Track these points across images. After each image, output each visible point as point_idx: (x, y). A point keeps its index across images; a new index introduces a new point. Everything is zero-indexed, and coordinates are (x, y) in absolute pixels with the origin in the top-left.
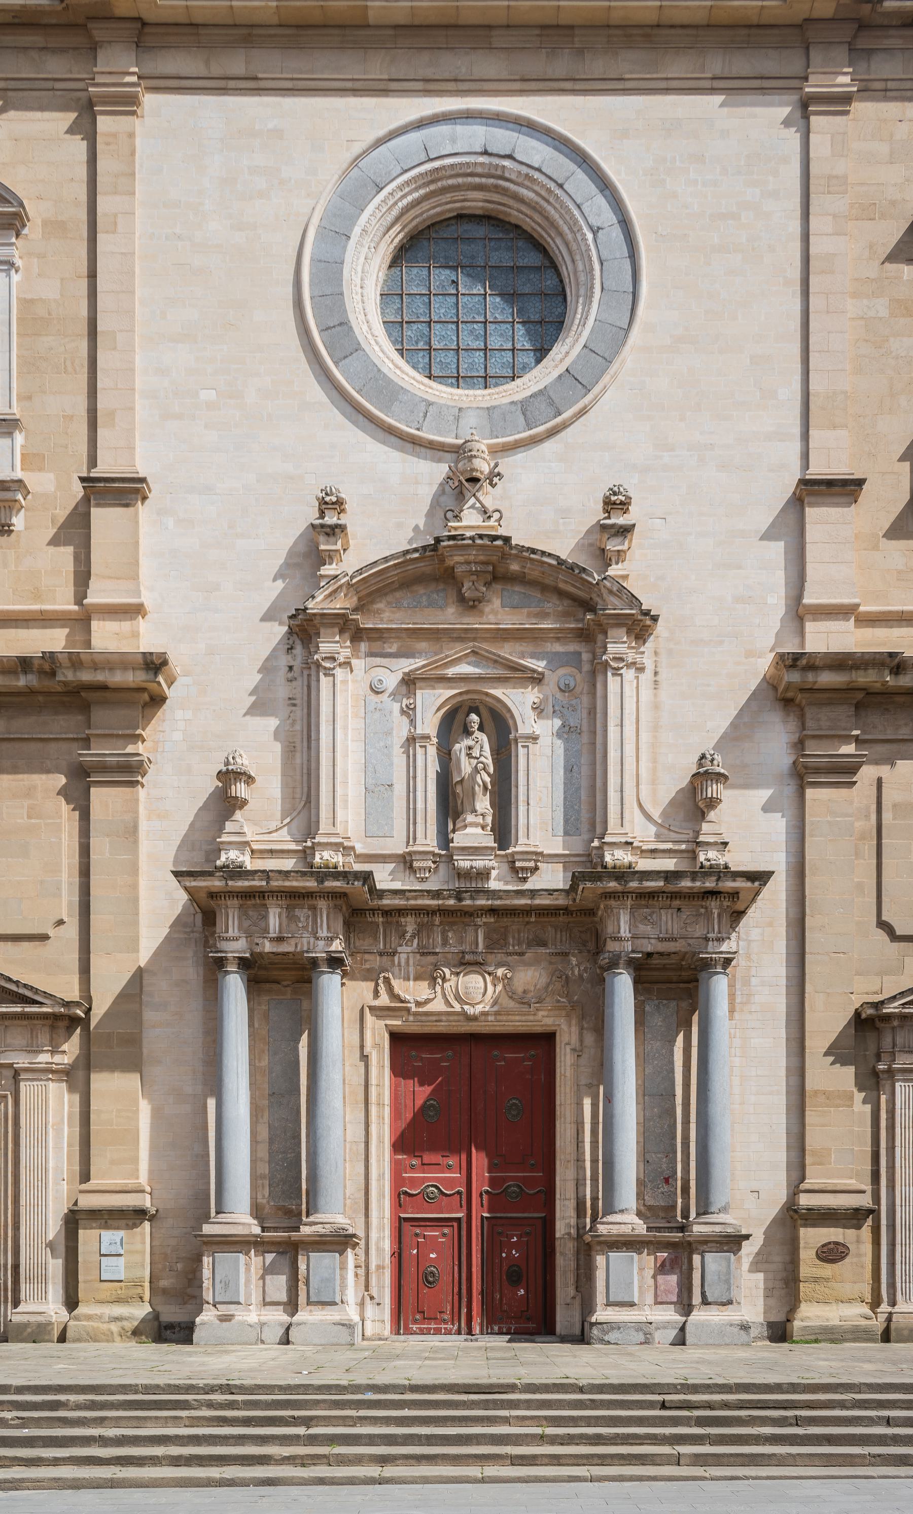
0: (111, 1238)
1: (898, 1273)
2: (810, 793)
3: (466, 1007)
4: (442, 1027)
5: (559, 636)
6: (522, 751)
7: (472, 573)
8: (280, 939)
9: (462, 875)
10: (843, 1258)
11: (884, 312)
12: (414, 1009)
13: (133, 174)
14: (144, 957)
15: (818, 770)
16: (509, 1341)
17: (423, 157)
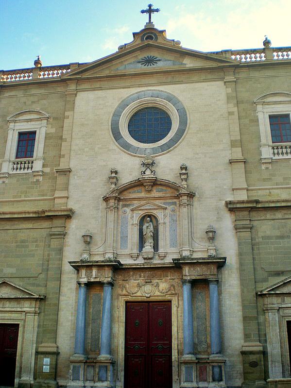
7: (147, 185)
8: (96, 278)
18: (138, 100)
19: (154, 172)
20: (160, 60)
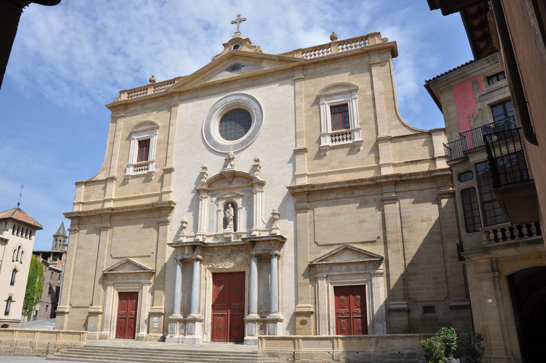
0: (156, 319)
1: (320, 327)
2: (298, 215)
3: (226, 267)
4: (222, 271)
5: (247, 187)
6: (239, 211)
9: (226, 238)
10: (306, 324)
11: (312, 114)
12: (216, 267)
13: (176, 116)
14: (167, 260)
15: (299, 210)
16: (235, 344)
17: (225, 103)
18: (226, 104)
19: (234, 166)
20: (243, 66)
